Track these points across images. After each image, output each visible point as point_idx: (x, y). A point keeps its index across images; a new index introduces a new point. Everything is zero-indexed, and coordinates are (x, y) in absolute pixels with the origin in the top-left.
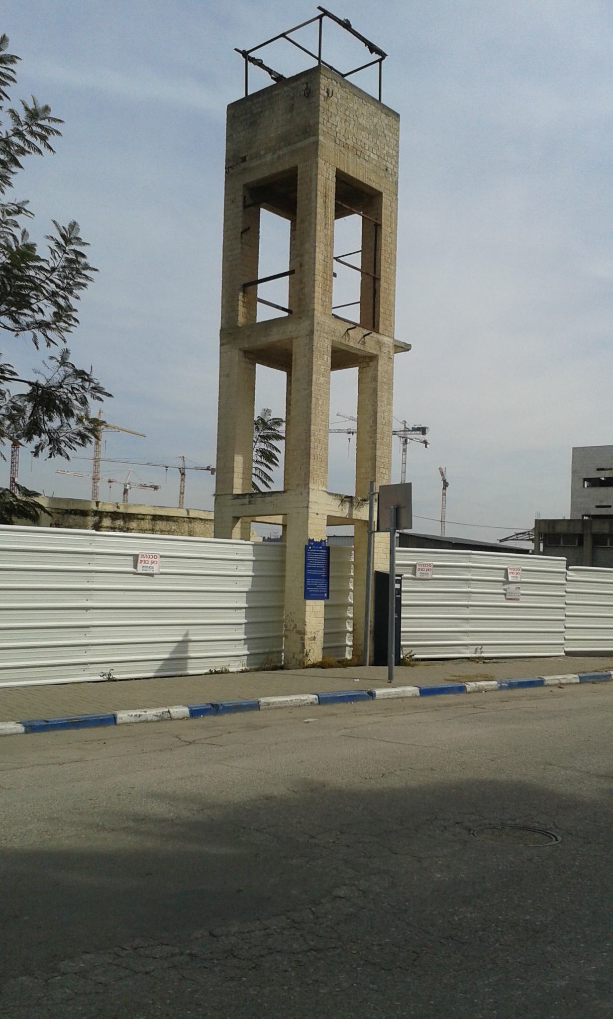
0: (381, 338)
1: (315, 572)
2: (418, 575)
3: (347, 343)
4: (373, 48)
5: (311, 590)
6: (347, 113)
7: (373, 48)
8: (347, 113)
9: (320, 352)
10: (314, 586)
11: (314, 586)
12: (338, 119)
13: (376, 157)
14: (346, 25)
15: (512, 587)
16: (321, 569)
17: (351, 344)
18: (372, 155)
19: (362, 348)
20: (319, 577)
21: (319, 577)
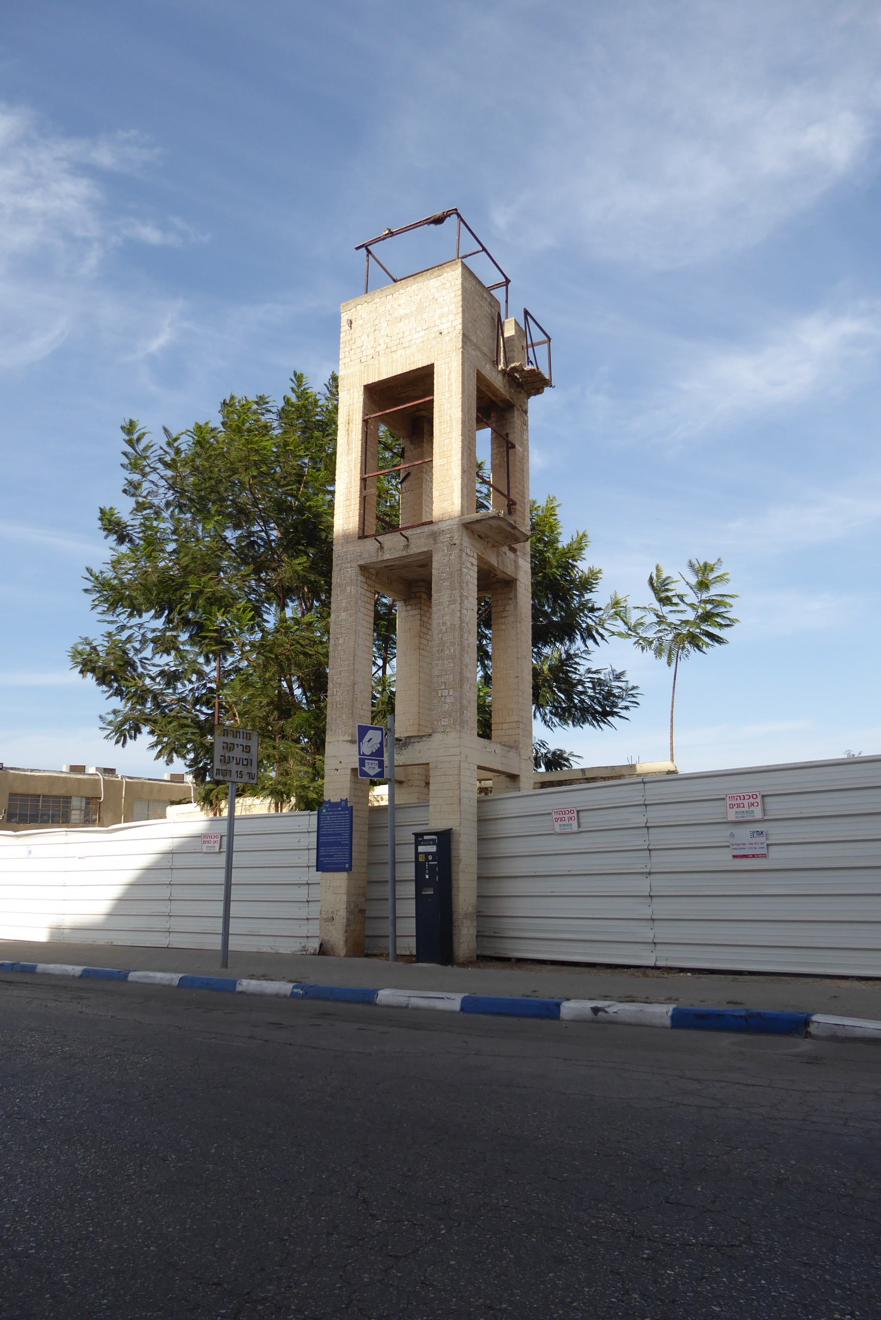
0: (435, 528)
1: (332, 839)
2: (558, 830)
3: (380, 559)
4: (438, 221)
5: (326, 860)
6: (377, 322)
7: (438, 221)
8: (377, 322)
9: (340, 585)
10: (332, 856)
11: (332, 856)
12: (363, 338)
13: (422, 333)
14: (391, 234)
15: (743, 834)
16: (340, 834)
17: (387, 556)
18: (415, 336)
19: (404, 553)
20: (338, 844)
21: (338, 844)
